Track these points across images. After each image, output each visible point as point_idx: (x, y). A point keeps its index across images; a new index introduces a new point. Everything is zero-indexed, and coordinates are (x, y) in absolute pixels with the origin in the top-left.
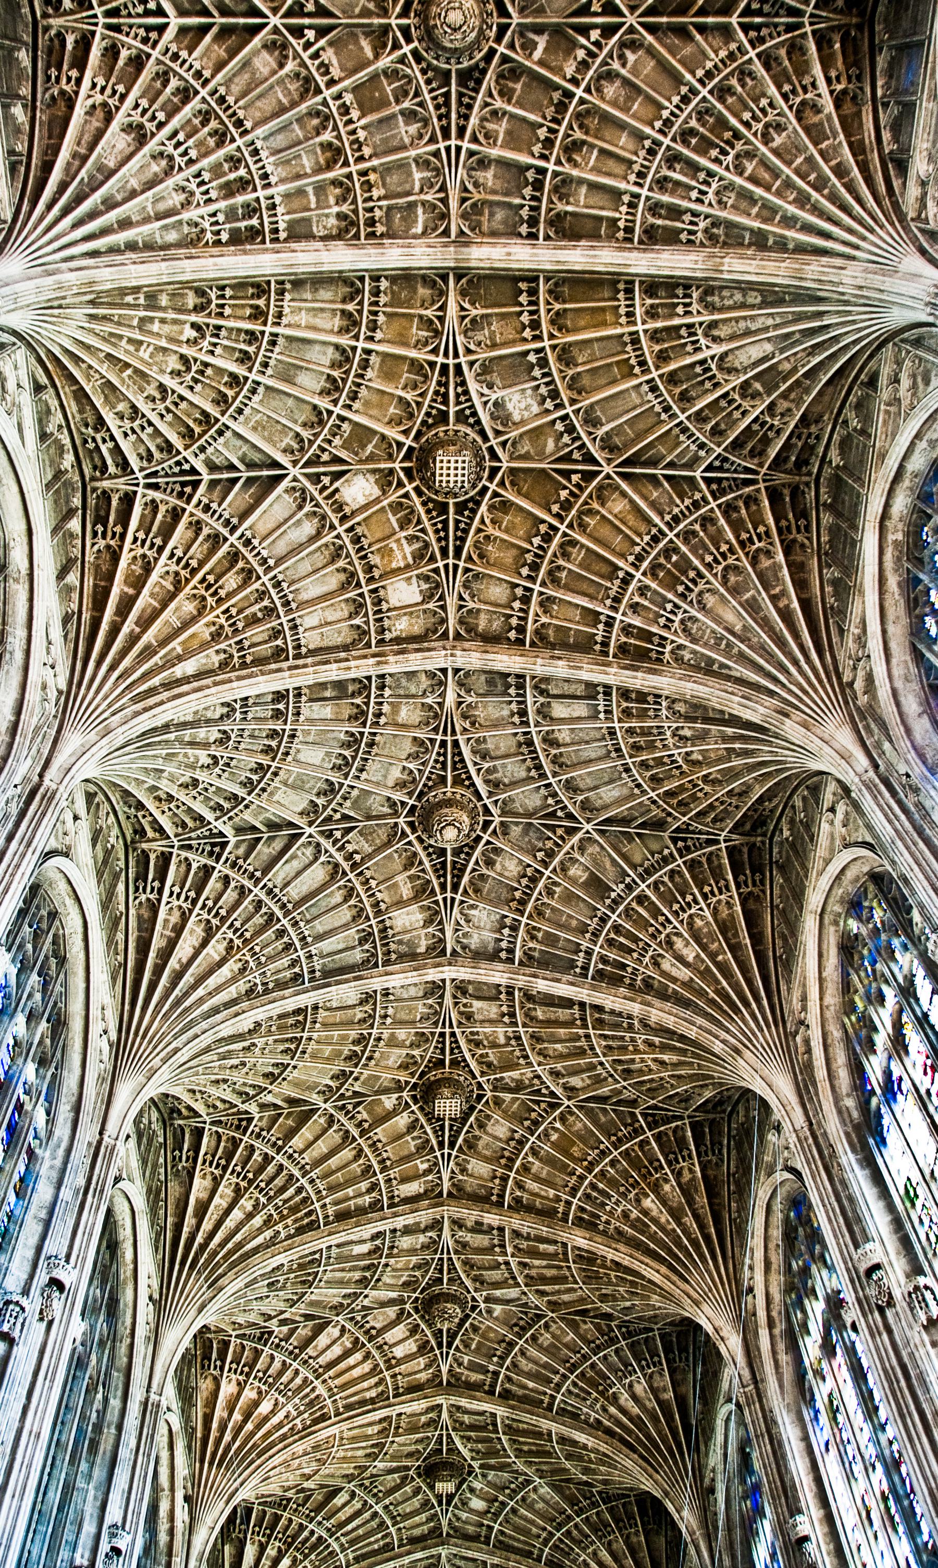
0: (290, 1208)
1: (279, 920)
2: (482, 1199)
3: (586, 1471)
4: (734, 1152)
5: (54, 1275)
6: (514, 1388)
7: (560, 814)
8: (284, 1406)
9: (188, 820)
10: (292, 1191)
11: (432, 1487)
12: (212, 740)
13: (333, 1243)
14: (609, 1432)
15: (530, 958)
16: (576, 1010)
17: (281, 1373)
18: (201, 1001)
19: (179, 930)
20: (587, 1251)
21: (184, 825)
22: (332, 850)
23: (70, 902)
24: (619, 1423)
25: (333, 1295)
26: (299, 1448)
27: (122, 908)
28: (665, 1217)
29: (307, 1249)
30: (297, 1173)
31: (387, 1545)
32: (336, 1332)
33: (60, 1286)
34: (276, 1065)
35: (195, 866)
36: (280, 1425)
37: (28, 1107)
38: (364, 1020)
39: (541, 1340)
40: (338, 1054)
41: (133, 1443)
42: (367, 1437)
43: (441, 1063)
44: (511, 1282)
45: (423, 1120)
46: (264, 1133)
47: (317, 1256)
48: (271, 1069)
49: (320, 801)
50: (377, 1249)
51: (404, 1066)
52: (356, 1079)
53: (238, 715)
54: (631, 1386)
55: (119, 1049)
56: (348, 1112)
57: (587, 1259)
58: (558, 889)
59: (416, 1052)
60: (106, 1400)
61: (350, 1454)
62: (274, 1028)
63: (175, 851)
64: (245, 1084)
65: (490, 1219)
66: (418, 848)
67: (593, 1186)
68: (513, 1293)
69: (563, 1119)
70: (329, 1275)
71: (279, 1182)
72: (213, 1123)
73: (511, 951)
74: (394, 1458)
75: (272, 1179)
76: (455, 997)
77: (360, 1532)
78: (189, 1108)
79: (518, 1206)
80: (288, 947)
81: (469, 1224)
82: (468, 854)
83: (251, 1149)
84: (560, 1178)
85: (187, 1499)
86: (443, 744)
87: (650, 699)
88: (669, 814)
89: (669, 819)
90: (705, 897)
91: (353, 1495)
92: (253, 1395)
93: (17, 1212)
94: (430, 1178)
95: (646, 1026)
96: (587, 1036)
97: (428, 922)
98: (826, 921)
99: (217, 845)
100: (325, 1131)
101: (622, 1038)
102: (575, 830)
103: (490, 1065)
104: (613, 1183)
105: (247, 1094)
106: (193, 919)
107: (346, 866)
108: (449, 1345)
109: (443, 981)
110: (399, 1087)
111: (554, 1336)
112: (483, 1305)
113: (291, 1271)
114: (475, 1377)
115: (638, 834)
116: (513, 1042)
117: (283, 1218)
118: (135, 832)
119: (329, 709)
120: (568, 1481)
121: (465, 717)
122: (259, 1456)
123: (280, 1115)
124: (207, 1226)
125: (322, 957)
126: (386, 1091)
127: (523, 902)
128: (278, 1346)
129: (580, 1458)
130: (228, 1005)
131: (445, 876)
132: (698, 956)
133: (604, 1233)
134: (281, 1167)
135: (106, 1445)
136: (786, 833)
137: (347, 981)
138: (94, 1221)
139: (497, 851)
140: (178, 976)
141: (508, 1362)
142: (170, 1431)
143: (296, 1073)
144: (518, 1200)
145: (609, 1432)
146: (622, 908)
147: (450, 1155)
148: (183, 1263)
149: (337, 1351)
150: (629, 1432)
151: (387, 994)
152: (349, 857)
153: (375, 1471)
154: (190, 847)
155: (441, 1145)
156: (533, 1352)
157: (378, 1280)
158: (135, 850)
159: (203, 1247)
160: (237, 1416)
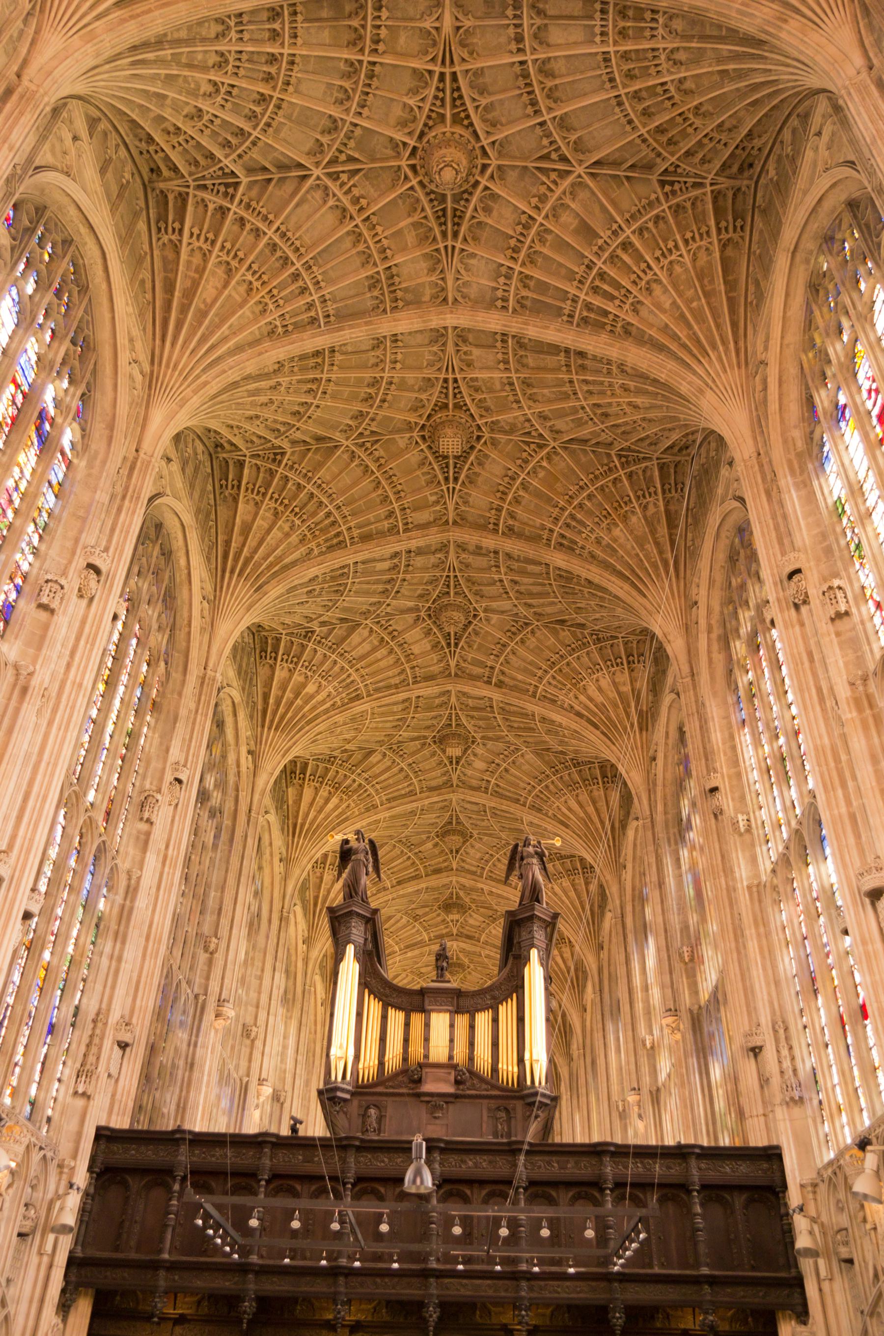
0: (321, 530)
1: (293, 264)
2: (481, 526)
3: (561, 743)
4: (694, 490)
5: (91, 561)
6: (506, 680)
7: (554, 156)
8: (325, 687)
9: (199, 158)
10: (322, 514)
11: (444, 751)
12: (210, 63)
13: (359, 559)
14: (579, 714)
15: (523, 306)
16: (562, 357)
17: (322, 663)
18: (224, 339)
19: (201, 271)
20: (566, 571)
21: (196, 163)
22: (339, 194)
23: (84, 230)
24: (587, 708)
25: (362, 602)
26: (339, 718)
27: (146, 247)
30: (325, 501)
31: (411, 791)
32: (366, 633)
33: (98, 571)
34: (302, 404)
35: (211, 207)
36: (323, 702)
37: (59, 420)
38: (377, 365)
39: (528, 643)
40: (353, 397)
41: (193, 706)
42: (394, 713)
43: (446, 406)
44: (505, 596)
45: (431, 458)
46: (296, 466)
47: (346, 570)
48: (297, 408)
49: (325, 140)
50: (395, 566)
51: (414, 409)
52: (373, 420)
53: (233, 35)
54: (597, 680)
55: (152, 381)
56: (366, 449)
57: (566, 577)
58: (549, 237)
59: (424, 396)
61: (380, 725)
62: (296, 369)
63: (191, 191)
64: (275, 421)
65: (489, 542)
66: (420, 193)
67: (572, 516)
68: (506, 605)
69: (549, 457)
70: (356, 586)
72: (252, 456)
73: (505, 300)
74: (415, 729)
76: (457, 345)
77: (391, 781)
78: (232, 444)
80: (304, 290)
81: (471, 548)
82: (467, 200)
85: (249, 752)
86: (442, 75)
87: (648, 15)
88: (659, 155)
89: (659, 160)
90: (686, 242)
91: (385, 755)
92: (301, 679)
93: (57, 511)
94: (438, 508)
95: (623, 371)
96: (571, 382)
97: (432, 270)
98: (798, 258)
99: (230, 185)
100: (349, 464)
101: (602, 383)
102: (569, 173)
103: (487, 409)
105: (278, 430)
106: (213, 260)
107: (352, 209)
108: (456, 645)
109: (445, 328)
110: (410, 427)
111: (538, 640)
112: (482, 615)
113: (325, 581)
114: (477, 671)
115: (628, 178)
116: (507, 388)
118: (152, 170)
119: (326, 33)
120: (548, 750)
121: (463, 44)
122: (309, 723)
123: (309, 450)
124: (251, 542)
125: (335, 301)
126: (399, 431)
127: (516, 250)
128: (319, 642)
129: (557, 733)
130: (253, 344)
131: (445, 224)
132: (674, 303)
136: (772, 173)
137: (358, 325)
139: (494, 197)
140: (202, 314)
141: (502, 659)
142: (233, 703)
143: (319, 413)
144: (510, 529)
145: (579, 714)
146: (606, 254)
147: (454, 488)
148: (232, 572)
149: (366, 647)
150: (594, 714)
151: (396, 341)
152: (356, 201)
153: (400, 739)
154: (205, 187)
155: (447, 479)
156: (521, 651)
157: (398, 592)
158: (153, 190)
160: (289, 694)
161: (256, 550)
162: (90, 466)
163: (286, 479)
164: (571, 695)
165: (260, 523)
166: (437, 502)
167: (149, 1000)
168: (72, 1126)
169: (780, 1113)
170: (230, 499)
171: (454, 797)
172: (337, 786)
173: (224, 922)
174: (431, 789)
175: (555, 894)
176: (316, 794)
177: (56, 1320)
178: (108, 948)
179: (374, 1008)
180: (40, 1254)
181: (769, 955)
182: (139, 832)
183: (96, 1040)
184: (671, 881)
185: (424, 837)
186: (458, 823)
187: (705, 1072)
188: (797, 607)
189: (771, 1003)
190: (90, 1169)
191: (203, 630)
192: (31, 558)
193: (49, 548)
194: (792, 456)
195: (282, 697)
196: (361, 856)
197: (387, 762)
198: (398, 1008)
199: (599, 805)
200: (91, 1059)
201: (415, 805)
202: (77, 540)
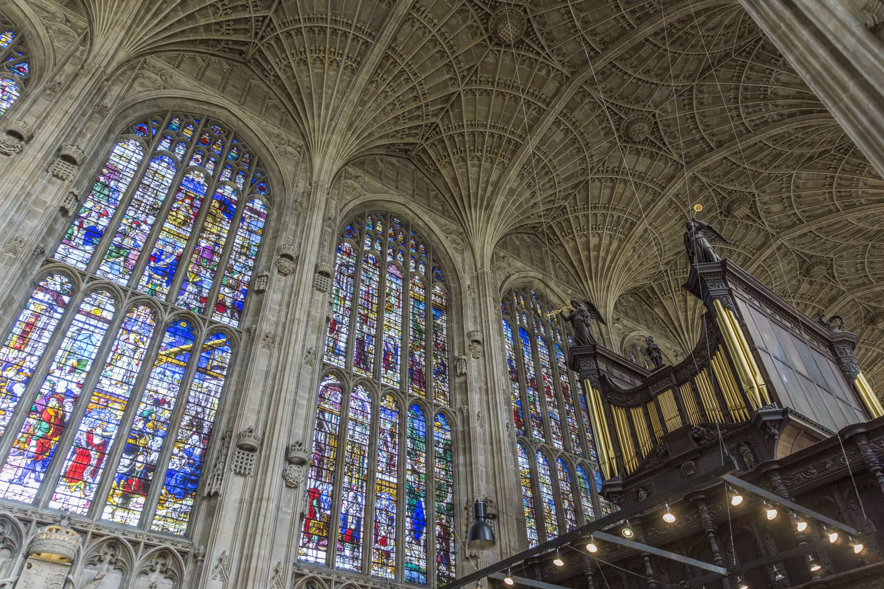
32: (597, 183)
92: (584, 239)
149: (607, 191)
156: (708, 110)
160: (583, 254)
163: (451, 137)
174: (760, 248)
185: (794, 282)
192: (250, 273)
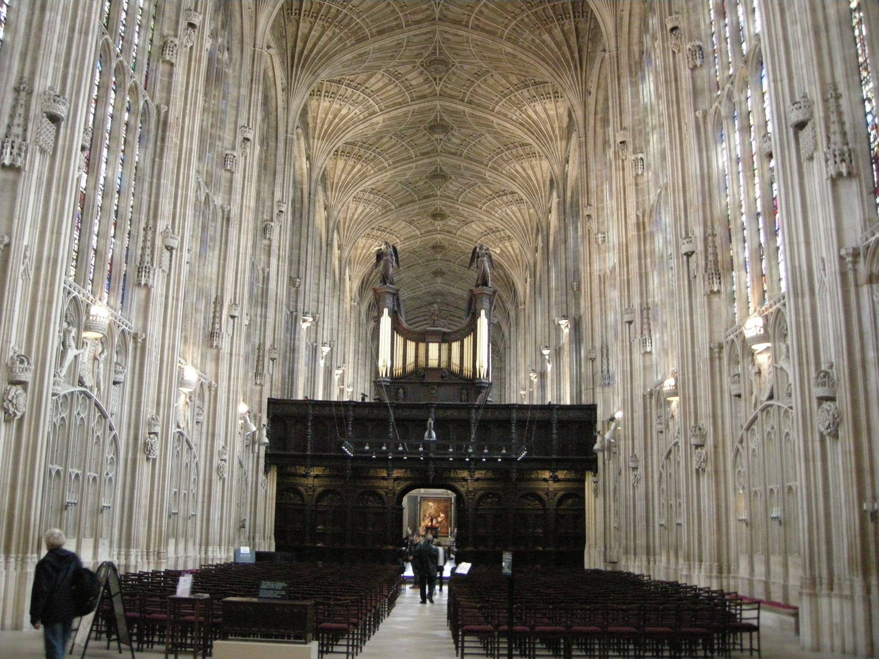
2: (457, 22)
14: (521, 124)
17: (351, 96)
24: (527, 122)
26: (361, 127)
28: (553, 45)
29: (362, 51)
32: (380, 76)
33: (248, 140)
36: (352, 118)
41: (282, 161)
60: (268, 143)
65: (460, 33)
71: (346, 21)
75: (342, 20)
79: (476, 28)
83: (330, 7)
84: (501, 20)
92: (338, 106)
94: (429, 12)
104: (527, 25)
114: (453, 93)
117: (349, 38)
124: (309, 46)
129: (508, 132)
133: (522, 47)
134: (346, 15)
135: (271, 166)
138: (258, 97)
141: (471, 89)
144: (477, 25)
145: (521, 124)
149: (380, 84)
156: (483, 86)
159: (308, 56)
160: (330, 116)
161: (311, 51)
162: (234, 71)
164: (517, 113)
165: (315, 34)
166: (428, 9)
167: (281, 334)
168: (256, 398)
169: (598, 390)
170: (294, 21)
171: (438, 159)
172: (359, 158)
173: (302, 268)
174: (423, 154)
175: (508, 214)
176: (346, 164)
177: (264, 478)
178: (259, 312)
179: (399, 340)
180: (253, 453)
181: (604, 312)
182: (265, 245)
183: (261, 358)
184: (571, 241)
186: (441, 170)
187: (578, 352)
188: (623, 160)
189: (602, 337)
190: (268, 417)
191: (284, 108)
193: (224, 133)
194: (632, 63)
195: (325, 118)
196: (389, 257)
197: (393, 142)
198: (411, 340)
199: (536, 170)
200: (260, 368)
201: (411, 165)
202: (236, 123)
